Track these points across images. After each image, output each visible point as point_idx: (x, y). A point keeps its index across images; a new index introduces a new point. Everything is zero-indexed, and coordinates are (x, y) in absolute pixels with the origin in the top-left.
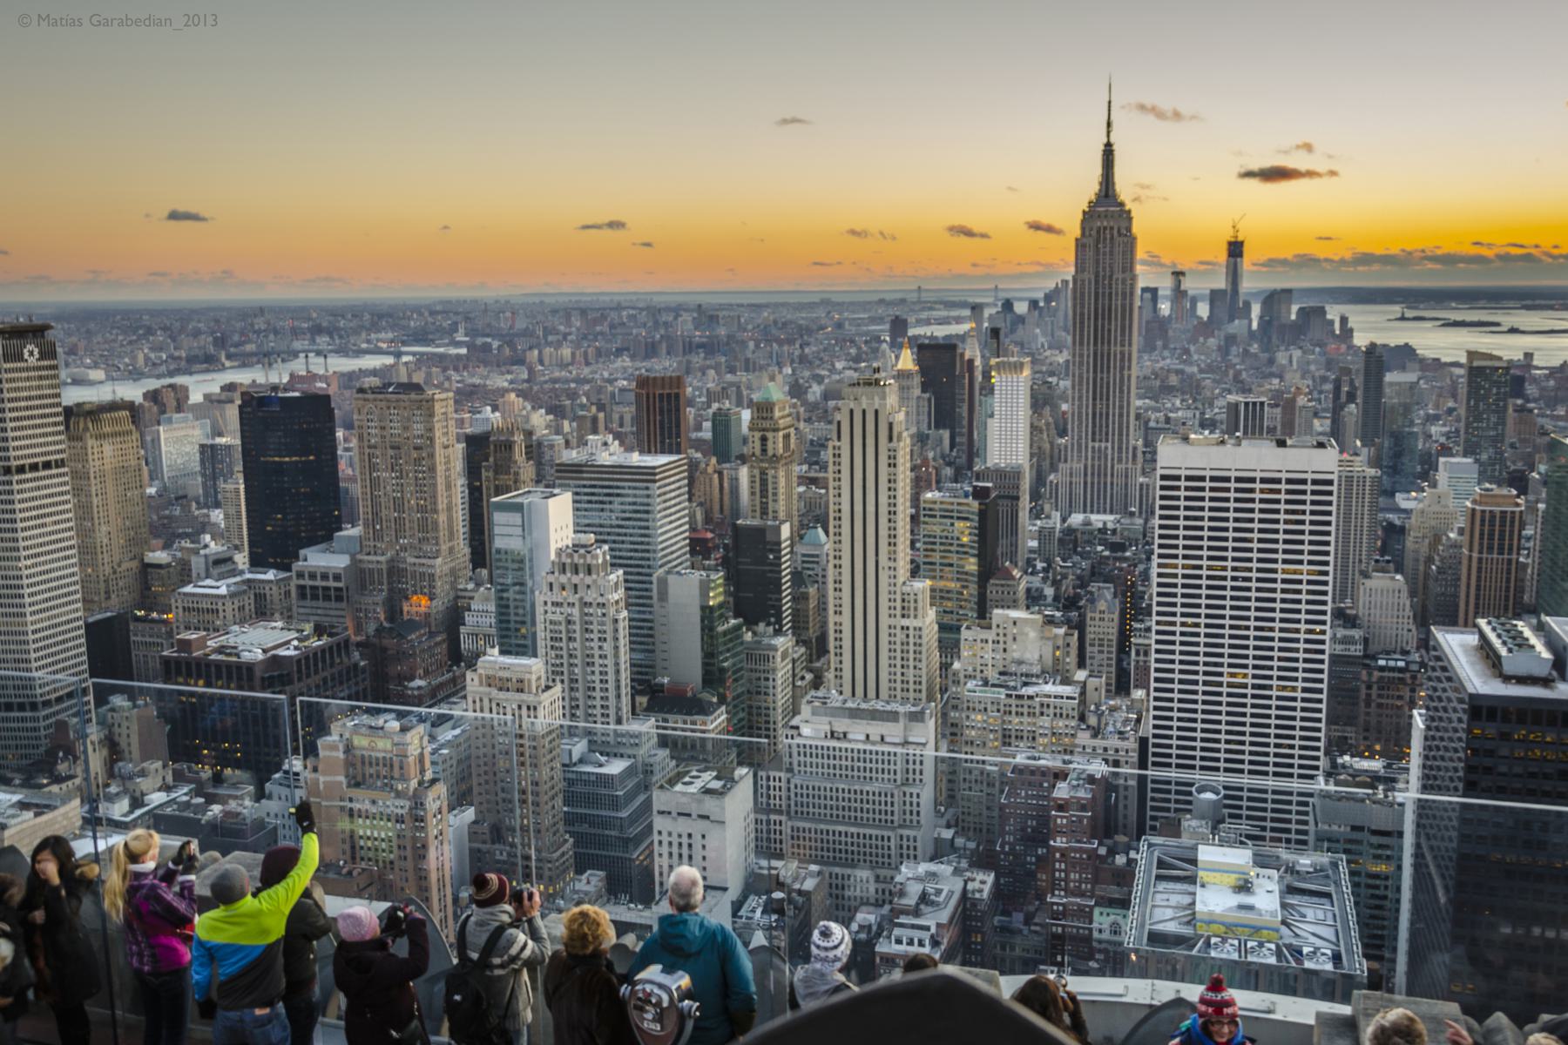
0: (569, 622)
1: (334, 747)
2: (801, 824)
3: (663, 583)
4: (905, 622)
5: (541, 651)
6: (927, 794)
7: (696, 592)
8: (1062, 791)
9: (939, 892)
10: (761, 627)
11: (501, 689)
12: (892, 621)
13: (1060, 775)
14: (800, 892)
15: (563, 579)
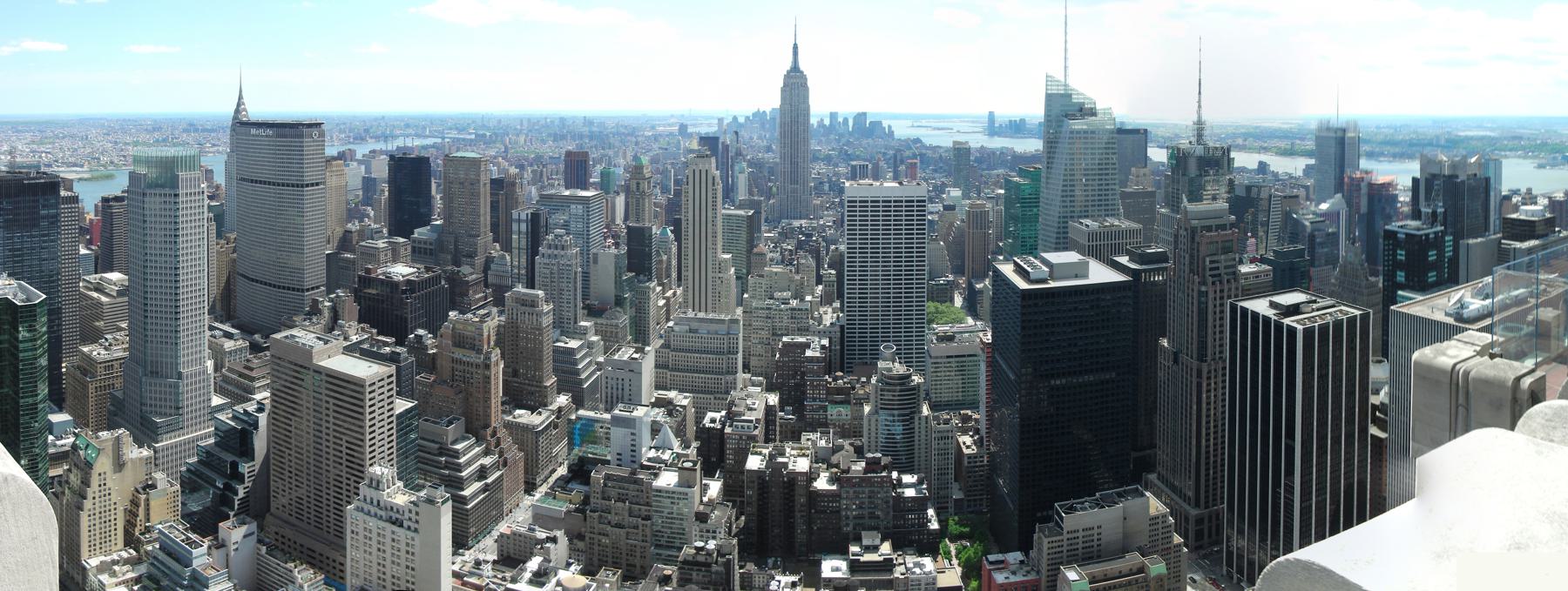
0: (552, 273)
1: (447, 328)
2: (676, 373)
3: (596, 255)
4: (721, 275)
5: (537, 286)
6: (740, 356)
7: (613, 260)
8: (809, 353)
9: (754, 404)
10: (641, 277)
11: (523, 305)
12: (714, 275)
13: (807, 346)
14: (681, 406)
15: (549, 252)
